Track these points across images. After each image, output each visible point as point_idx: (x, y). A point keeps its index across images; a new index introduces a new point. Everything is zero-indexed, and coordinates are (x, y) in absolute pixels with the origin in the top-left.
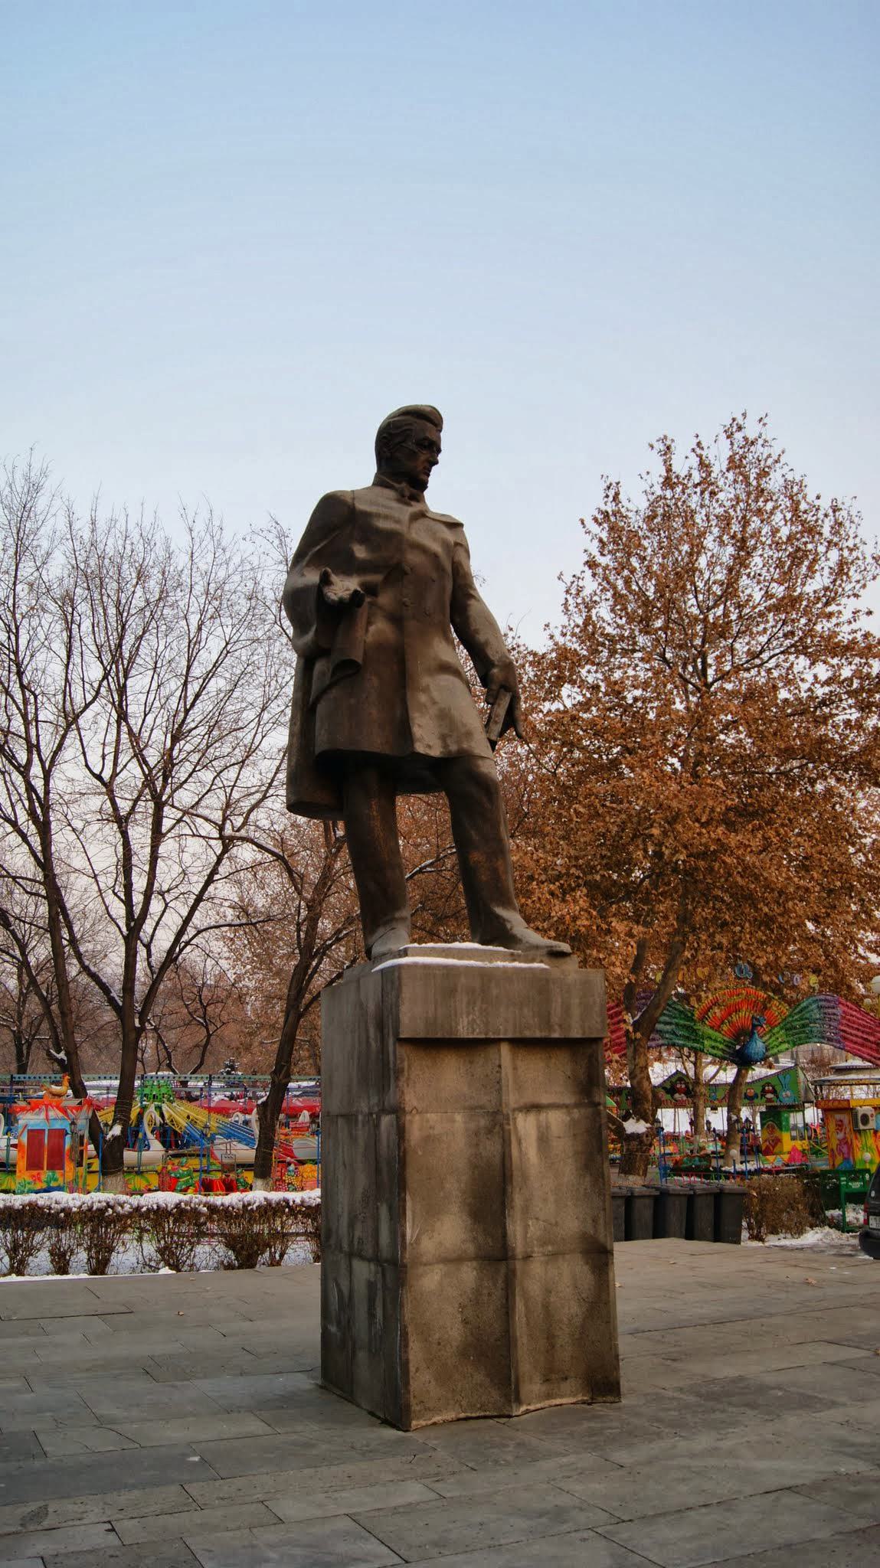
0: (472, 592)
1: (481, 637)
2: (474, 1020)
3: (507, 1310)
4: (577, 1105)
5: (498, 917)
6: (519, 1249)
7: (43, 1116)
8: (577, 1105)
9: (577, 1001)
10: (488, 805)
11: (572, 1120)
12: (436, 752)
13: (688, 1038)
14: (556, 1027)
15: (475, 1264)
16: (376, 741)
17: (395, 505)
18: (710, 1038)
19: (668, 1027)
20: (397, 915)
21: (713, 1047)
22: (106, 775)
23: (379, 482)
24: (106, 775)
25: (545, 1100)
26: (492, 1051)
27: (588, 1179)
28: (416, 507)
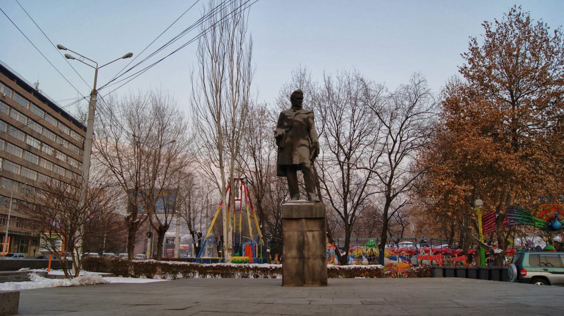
1: (312, 137)
3: (303, 267)
8: (321, 230)
12: (298, 163)
13: (528, 222)
16: (287, 163)
17: (292, 113)
18: (537, 221)
19: (520, 218)
21: (539, 225)
22: (336, 152)
23: (292, 108)
24: (336, 152)
25: (314, 229)
26: (302, 220)
28: (298, 111)
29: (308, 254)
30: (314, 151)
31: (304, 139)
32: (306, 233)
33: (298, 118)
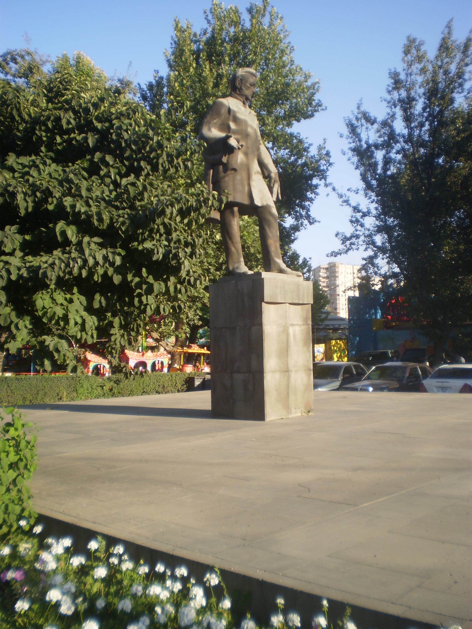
4: (303, 325)
5: (277, 263)
8: (303, 325)
25: (295, 322)
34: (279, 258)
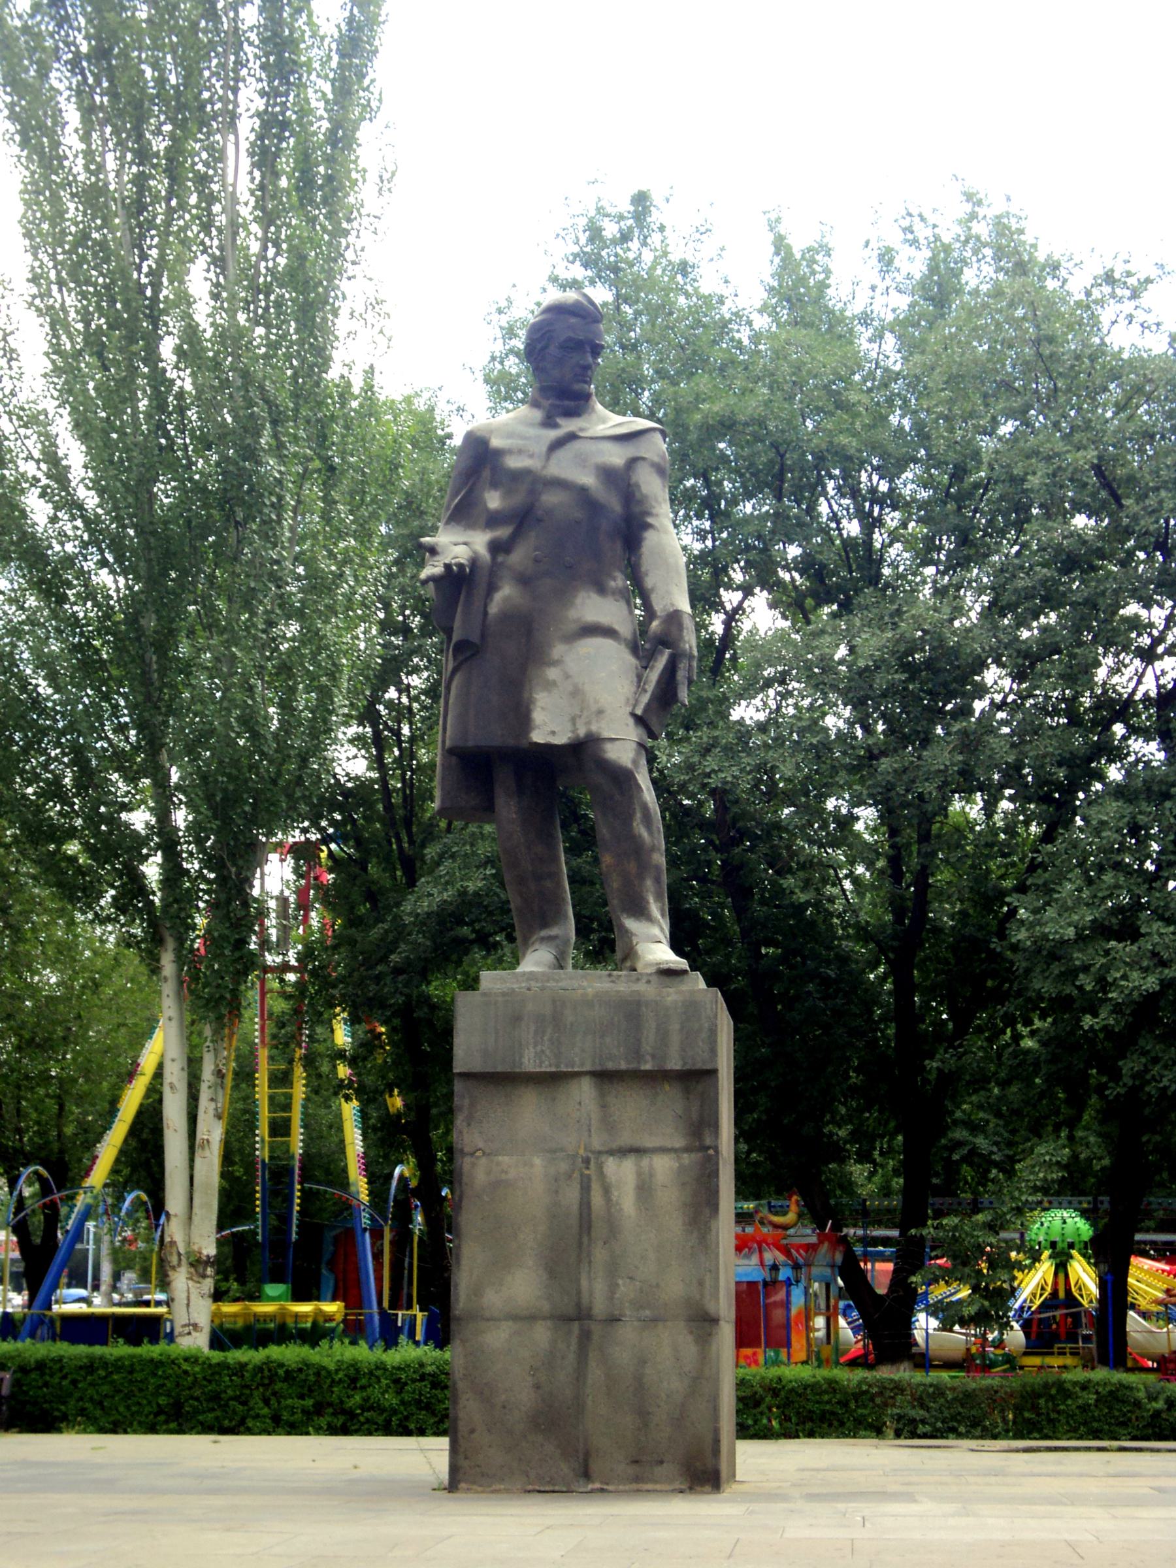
0: (650, 520)
2: (543, 1051)
3: (580, 1374)
6: (599, 1307)
7: (755, 1259)
8: (688, 1149)
9: (677, 1027)
10: (617, 797)
11: (682, 1169)
12: (561, 740)
14: (648, 1058)
15: (549, 1323)
16: (494, 736)
20: (544, 933)
25: (649, 1142)
27: (695, 1234)
28: (568, 425)
29: (611, 1297)
30: (661, 663)
31: (602, 590)
32: (600, 1167)
33: (563, 467)
34: (640, 912)
